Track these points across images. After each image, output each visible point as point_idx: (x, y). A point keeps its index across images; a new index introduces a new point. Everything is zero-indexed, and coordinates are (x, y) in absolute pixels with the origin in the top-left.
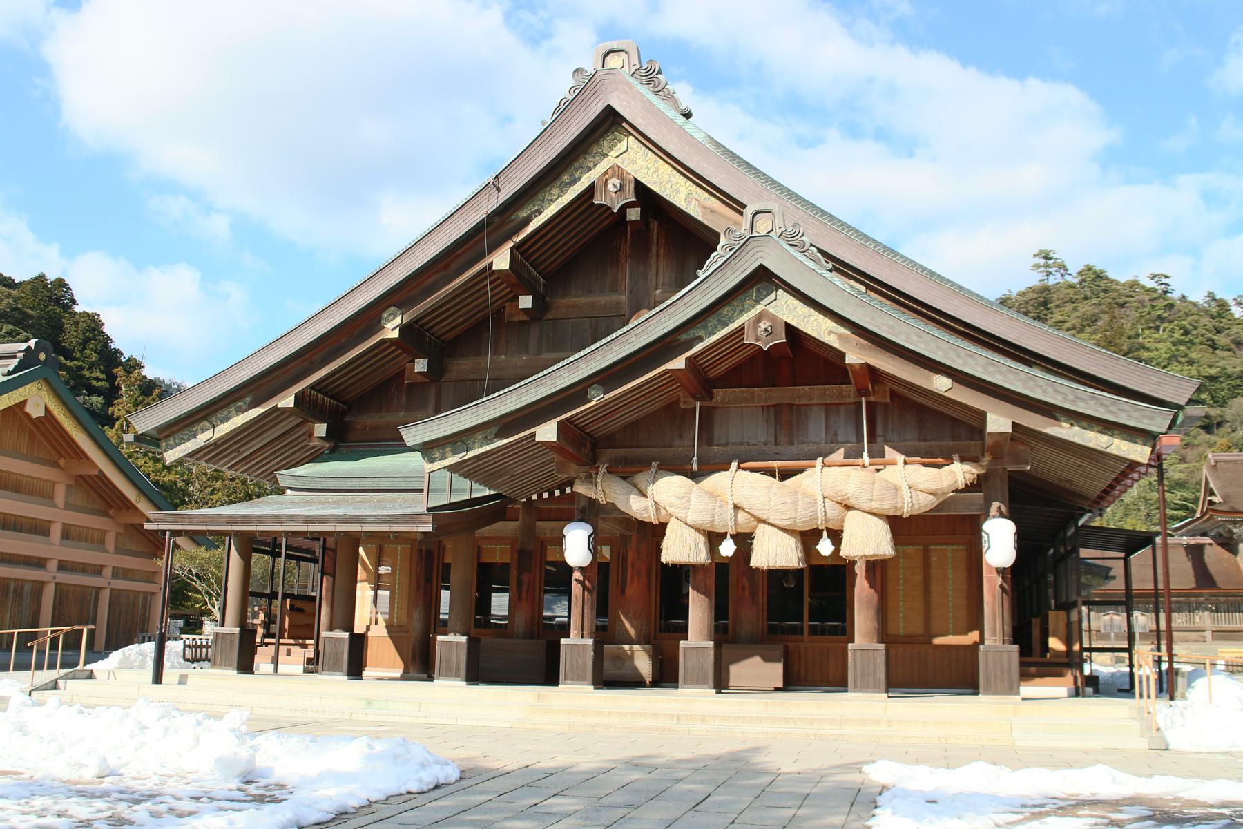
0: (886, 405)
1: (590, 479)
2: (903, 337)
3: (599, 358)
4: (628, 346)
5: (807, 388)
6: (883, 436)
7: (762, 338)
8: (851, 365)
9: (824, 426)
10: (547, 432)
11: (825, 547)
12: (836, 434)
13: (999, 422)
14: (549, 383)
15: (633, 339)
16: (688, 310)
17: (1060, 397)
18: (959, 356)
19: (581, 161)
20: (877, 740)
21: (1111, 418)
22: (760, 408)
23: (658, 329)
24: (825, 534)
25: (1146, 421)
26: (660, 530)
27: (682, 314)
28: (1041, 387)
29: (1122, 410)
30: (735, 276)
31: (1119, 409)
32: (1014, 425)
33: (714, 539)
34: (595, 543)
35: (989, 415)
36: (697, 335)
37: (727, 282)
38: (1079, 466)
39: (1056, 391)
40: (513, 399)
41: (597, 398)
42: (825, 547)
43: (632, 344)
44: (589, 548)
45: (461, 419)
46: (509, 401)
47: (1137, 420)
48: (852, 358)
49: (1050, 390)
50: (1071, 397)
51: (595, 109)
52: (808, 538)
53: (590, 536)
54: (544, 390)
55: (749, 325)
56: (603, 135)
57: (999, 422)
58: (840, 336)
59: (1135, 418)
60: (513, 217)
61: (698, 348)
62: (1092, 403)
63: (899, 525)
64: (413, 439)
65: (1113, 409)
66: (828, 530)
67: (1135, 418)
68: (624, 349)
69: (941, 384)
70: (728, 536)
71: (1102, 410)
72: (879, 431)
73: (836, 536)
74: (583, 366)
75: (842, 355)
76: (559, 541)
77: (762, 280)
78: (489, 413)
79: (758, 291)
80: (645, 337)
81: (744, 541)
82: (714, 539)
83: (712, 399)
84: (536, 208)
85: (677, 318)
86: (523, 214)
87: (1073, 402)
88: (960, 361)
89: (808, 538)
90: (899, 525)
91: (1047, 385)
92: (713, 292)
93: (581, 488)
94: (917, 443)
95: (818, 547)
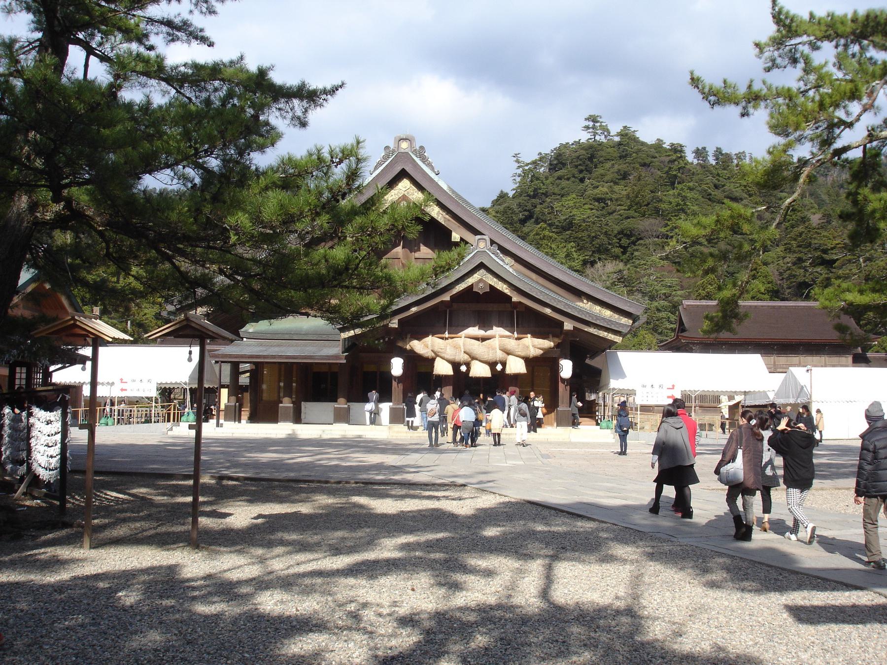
7: (480, 289)
11: (499, 367)
13: (568, 325)
21: (608, 327)
26: (433, 360)
34: (406, 367)
41: (414, 309)
42: (499, 367)
48: (514, 299)
51: (398, 169)
52: (492, 365)
57: (568, 325)
63: (529, 361)
69: (548, 311)
72: (520, 322)
73: (504, 364)
76: (389, 364)
77: (481, 266)
89: (492, 365)
90: (529, 361)
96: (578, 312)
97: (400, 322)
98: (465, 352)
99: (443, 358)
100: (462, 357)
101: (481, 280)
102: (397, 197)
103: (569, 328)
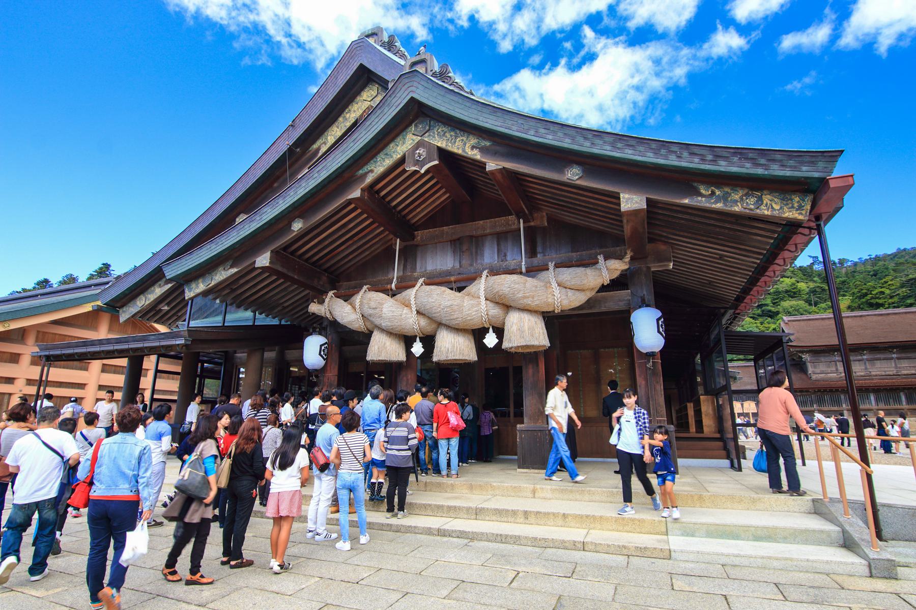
0: (544, 228)
1: (322, 302)
2: (532, 132)
3: (292, 194)
4: (313, 181)
5: (481, 222)
6: (543, 252)
8: (492, 172)
9: (496, 250)
10: (263, 260)
11: (490, 340)
12: (505, 255)
14: (258, 219)
15: (316, 175)
16: (356, 145)
17: (696, 160)
18: (586, 138)
19: (350, 107)
20: (504, 540)
22: (449, 243)
23: (334, 164)
24: (491, 330)
25: (804, 168)
27: (352, 149)
28: (675, 152)
29: (774, 160)
30: (391, 110)
31: (769, 160)
32: (649, 201)
33: (408, 341)
34: (326, 352)
35: (621, 195)
36: (369, 169)
37: (385, 117)
38: (721, 257)
39: (692, 154)
40: (234, 234)
42: (490, 340)
43: (315, 180)
44: (320, 354)
45: (201, 254)
46: (231, 236)
47: (794, 168)
48: (492, 165)
49: (685, 154)
50: (710, 157)
52: (478, 334)
53: (321, 346)
54: (255, 224)
55: (409, 154)
56: (362, 89)
58: (483, 150)
59: (790, 167)
60: (310, 149)
61: (369, 179)
62: (736, 159)
64: (170, 273)
65: (763, 161)
66: (493, 327)
67: (790, 167)
68: (310, 184)
70: (418, 339)
71: (748, 165)
72: (539, 249)
73: (500, 332)
74: (281, 202)
75: (482, 165)
78: (218, 248)
79: (416, 126)
80: (325, 172)
81: (429, 341)
82: (408, 341)
83: (414, 239)
84: (324, 140)
85: (348, 152)
86: (315, 146)
87: (714, 161)
88: (588, 144)
89: (478, 334)
91: (681, 148)
92: (375, 127)
93: (314, 308)
94: (570, 254)
95: (484, 341)
96: (656, 152)
97: (276, 254)
98: (418, 312)
99: (382, 330)
100: (411, 322)
101: (418, 145)
102: (361, 112)
103: (635, 206)
